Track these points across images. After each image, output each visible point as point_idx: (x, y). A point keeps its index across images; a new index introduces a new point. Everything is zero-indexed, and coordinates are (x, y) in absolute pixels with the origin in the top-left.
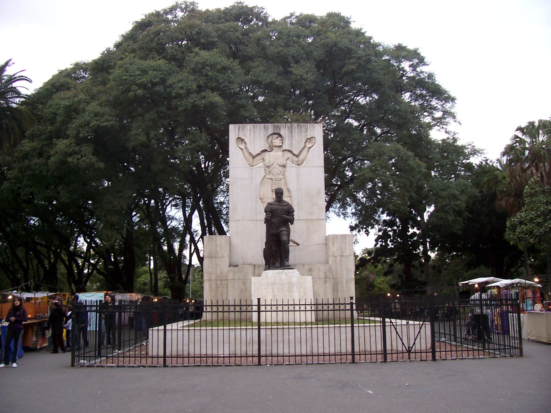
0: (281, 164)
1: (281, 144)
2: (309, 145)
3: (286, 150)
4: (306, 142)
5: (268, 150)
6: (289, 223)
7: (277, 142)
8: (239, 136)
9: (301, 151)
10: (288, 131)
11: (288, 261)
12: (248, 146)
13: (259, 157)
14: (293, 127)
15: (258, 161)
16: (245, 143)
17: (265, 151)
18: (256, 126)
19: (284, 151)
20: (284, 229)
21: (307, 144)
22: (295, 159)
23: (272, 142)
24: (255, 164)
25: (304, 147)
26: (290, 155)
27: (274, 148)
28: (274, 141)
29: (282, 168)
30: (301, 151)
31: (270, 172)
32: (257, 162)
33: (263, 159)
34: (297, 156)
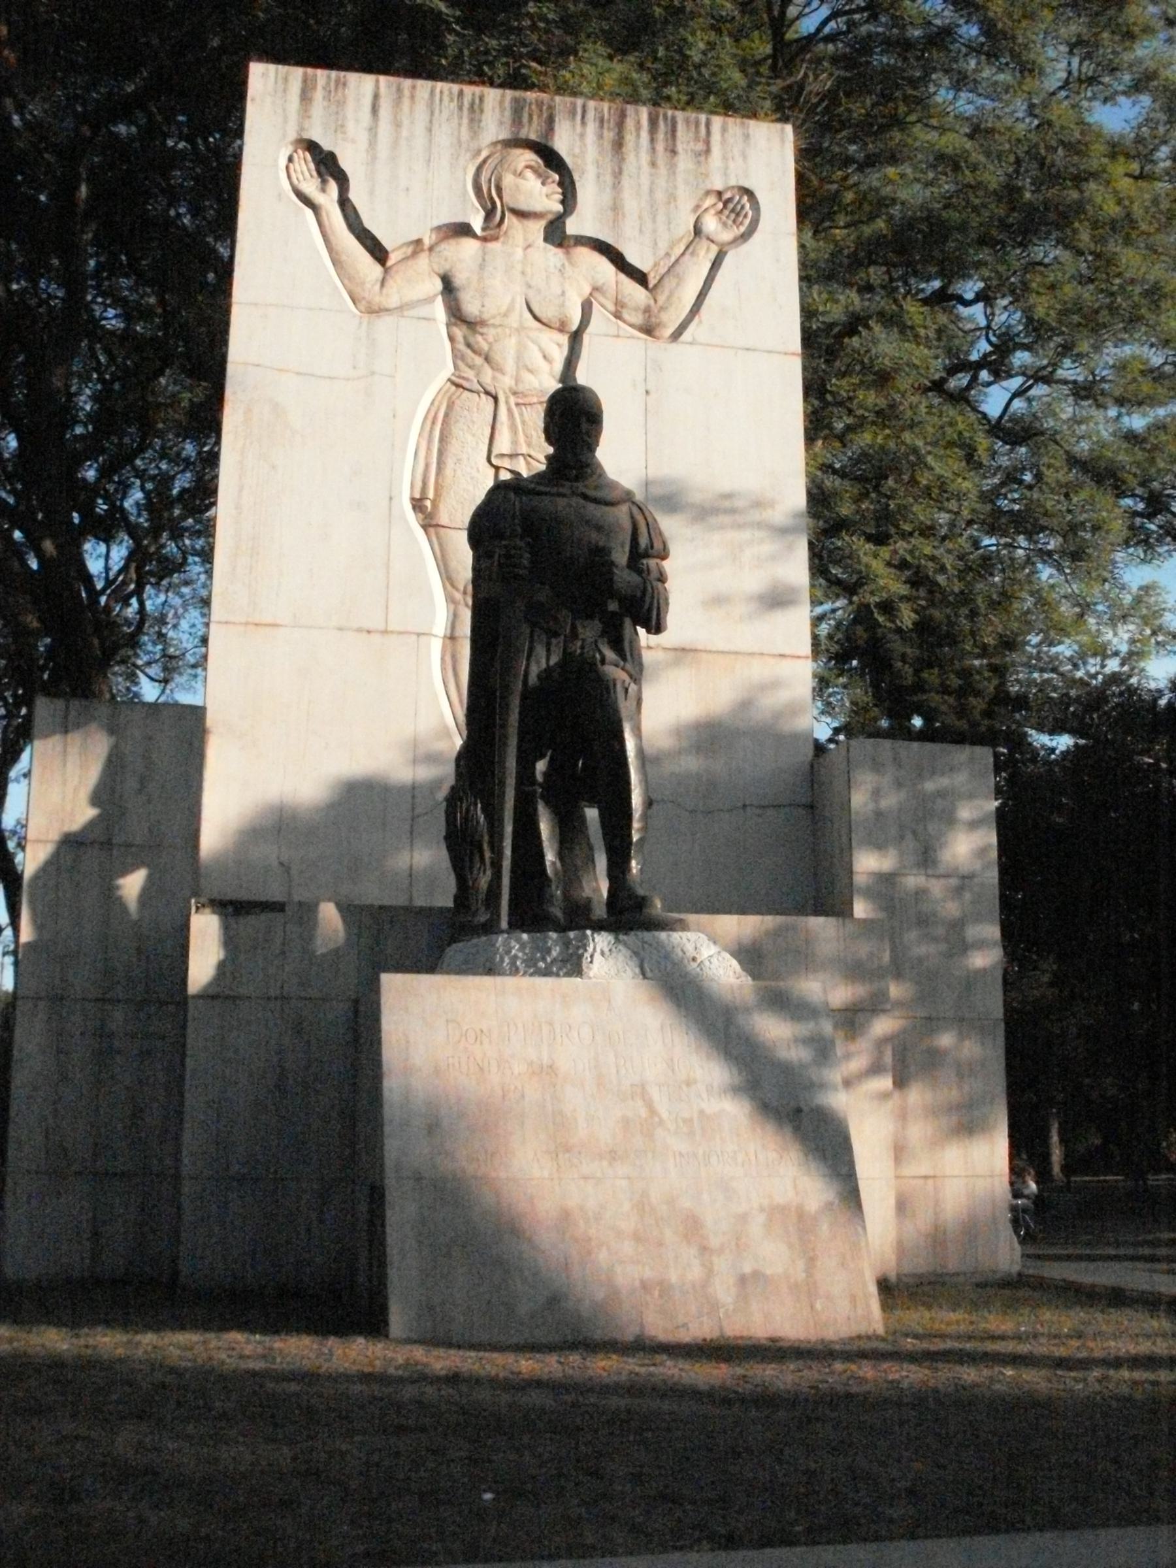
3: (581, 241)
5: (478, 231)
8: (302, 129)
10: (601, 137)
12: (356, 195)
14: (630, 123)
18: (414, 87)
22: (635, 292)
26: (606, 268)
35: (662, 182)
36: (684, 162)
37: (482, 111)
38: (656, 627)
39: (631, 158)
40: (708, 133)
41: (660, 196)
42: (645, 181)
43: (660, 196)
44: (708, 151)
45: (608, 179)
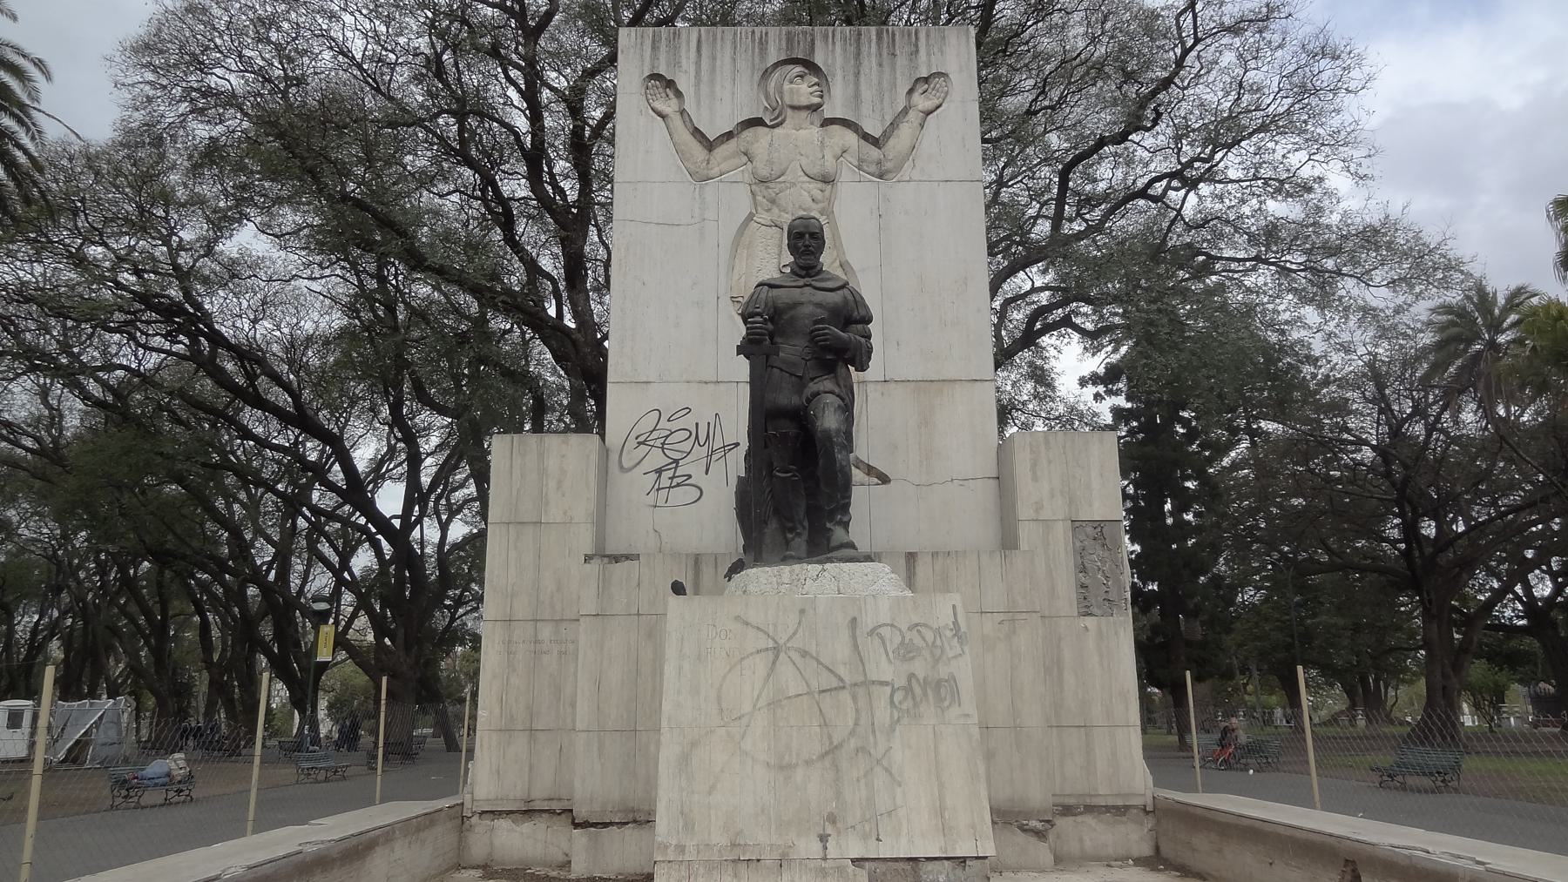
0: (814, 171)
1: (816, 100)
2: (921, 102)
4: (911, 91)
6: (852, 369)
7: (804, 91)
9: (894, 125)
11: (846, 525)
12: (689, 105)
13: (732, 145)
15: (725, 159)
16: (679, 94)
17: (756, 122)
19: (827, 122)
20: (827, 384)
21: (916, 97)
22: (874, 153)
23: (781, 93)
24: (716, 171)
25: (905, 111)
26: (851, 138)
27: (789, 112)
28: (787, 86)
29: (820, 185)
30: (894, 125)
31: (773, 201)
32: (724, 167)
33: (746, 154)
34: (875, 142)
35: (887, 76)
36: (901, 61)
37: (767, 43)
38: (862, 367)
39: (865, 63)
40: (917, 39)
41: (885, 85)
42: (874, 77)
43: (885, 85)
44: (917, 51)
45: (851, 77)
